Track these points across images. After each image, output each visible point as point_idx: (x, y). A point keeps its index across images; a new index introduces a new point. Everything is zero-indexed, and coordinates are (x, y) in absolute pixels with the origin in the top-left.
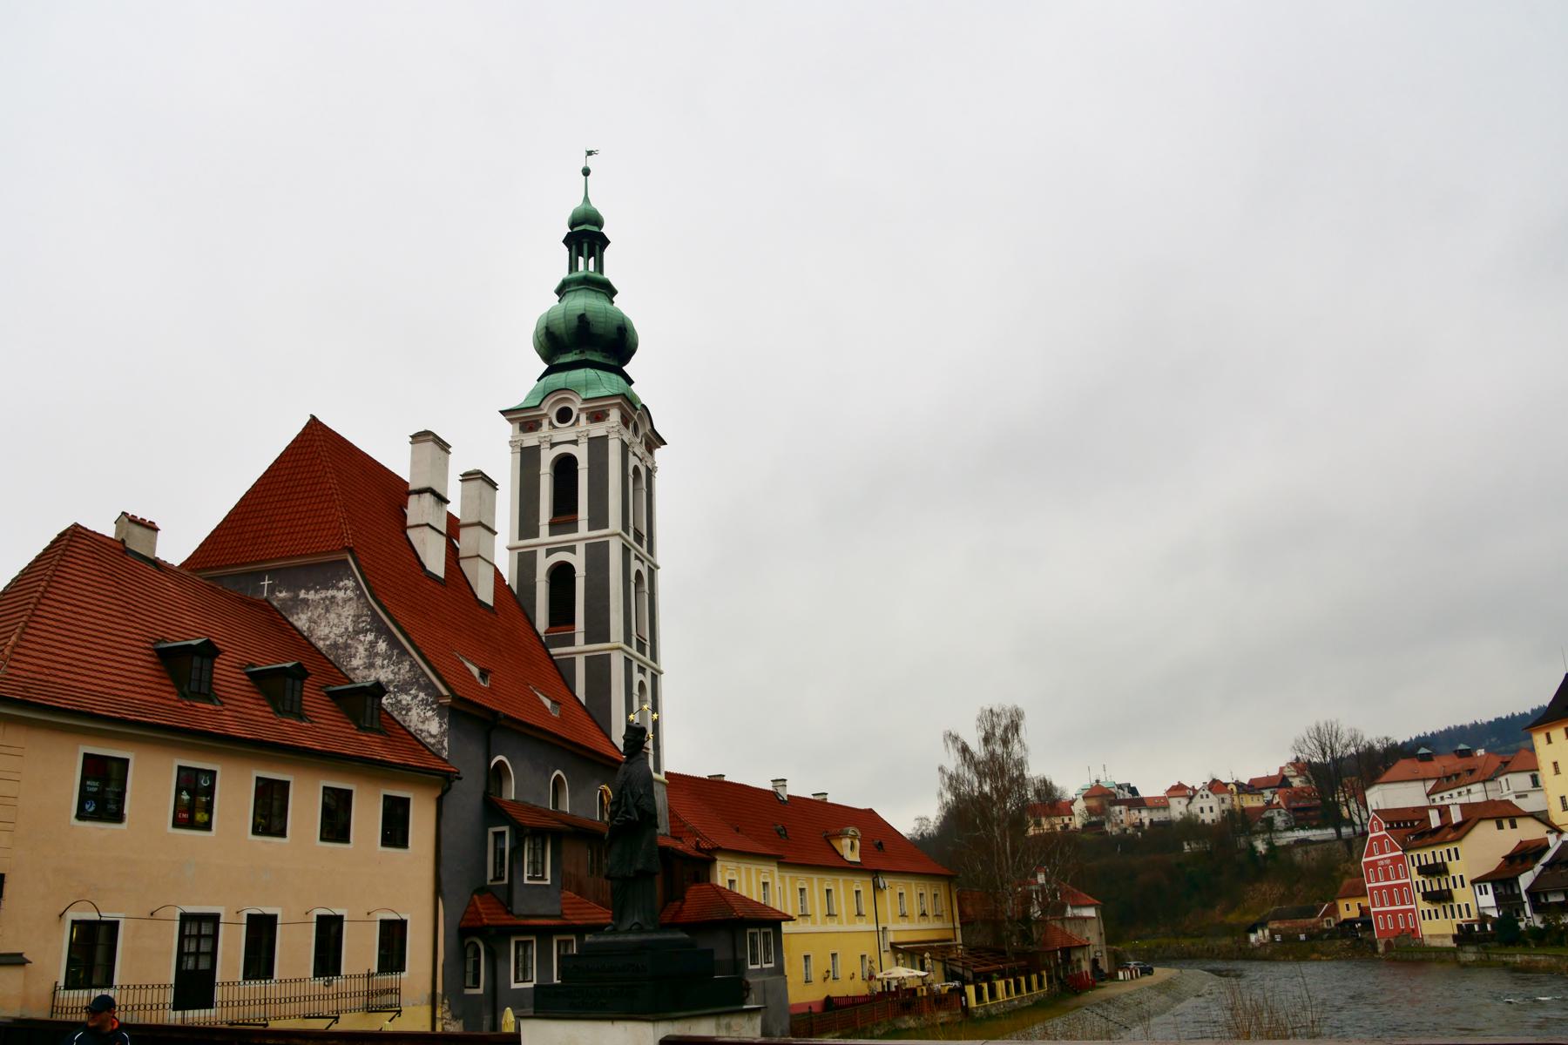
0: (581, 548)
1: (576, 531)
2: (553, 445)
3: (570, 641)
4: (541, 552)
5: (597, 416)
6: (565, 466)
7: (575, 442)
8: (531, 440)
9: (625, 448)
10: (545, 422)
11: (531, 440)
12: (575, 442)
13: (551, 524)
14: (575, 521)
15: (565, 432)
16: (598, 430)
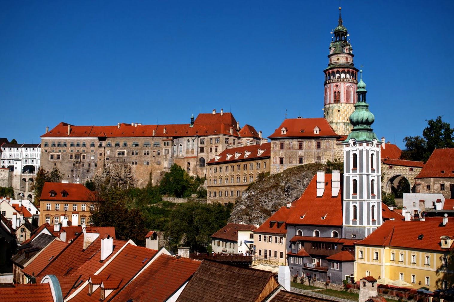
0: (358, 176)
1: (357, 172)
2: (352, 151)
3: (357, 198)
4: (351, 176)
5: (361, 144)
6: (355, 155)
7: (356, 150)
8: (347, 149)
9: (368, 151)
10: (350, 145)
11: (347, 149)
12: (356, 150)
13: (352, 170)
14: (356, 170)
15: (354, 148)
16: (360, 148)
